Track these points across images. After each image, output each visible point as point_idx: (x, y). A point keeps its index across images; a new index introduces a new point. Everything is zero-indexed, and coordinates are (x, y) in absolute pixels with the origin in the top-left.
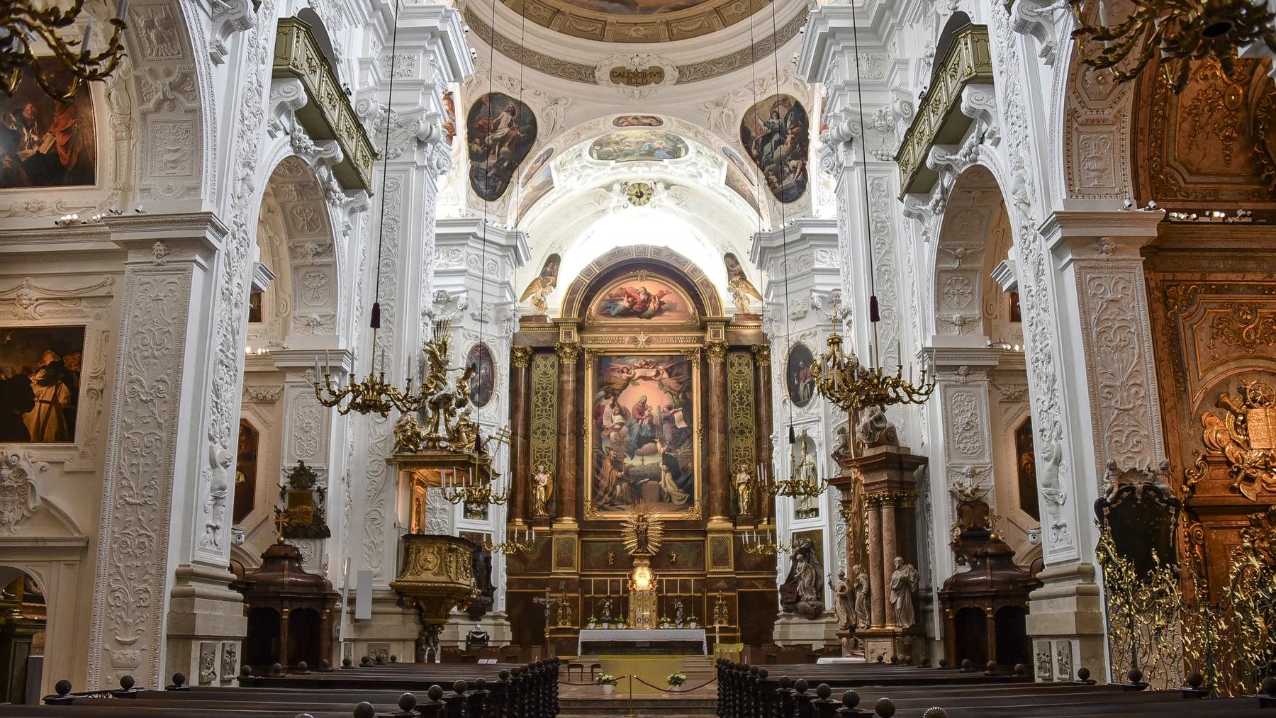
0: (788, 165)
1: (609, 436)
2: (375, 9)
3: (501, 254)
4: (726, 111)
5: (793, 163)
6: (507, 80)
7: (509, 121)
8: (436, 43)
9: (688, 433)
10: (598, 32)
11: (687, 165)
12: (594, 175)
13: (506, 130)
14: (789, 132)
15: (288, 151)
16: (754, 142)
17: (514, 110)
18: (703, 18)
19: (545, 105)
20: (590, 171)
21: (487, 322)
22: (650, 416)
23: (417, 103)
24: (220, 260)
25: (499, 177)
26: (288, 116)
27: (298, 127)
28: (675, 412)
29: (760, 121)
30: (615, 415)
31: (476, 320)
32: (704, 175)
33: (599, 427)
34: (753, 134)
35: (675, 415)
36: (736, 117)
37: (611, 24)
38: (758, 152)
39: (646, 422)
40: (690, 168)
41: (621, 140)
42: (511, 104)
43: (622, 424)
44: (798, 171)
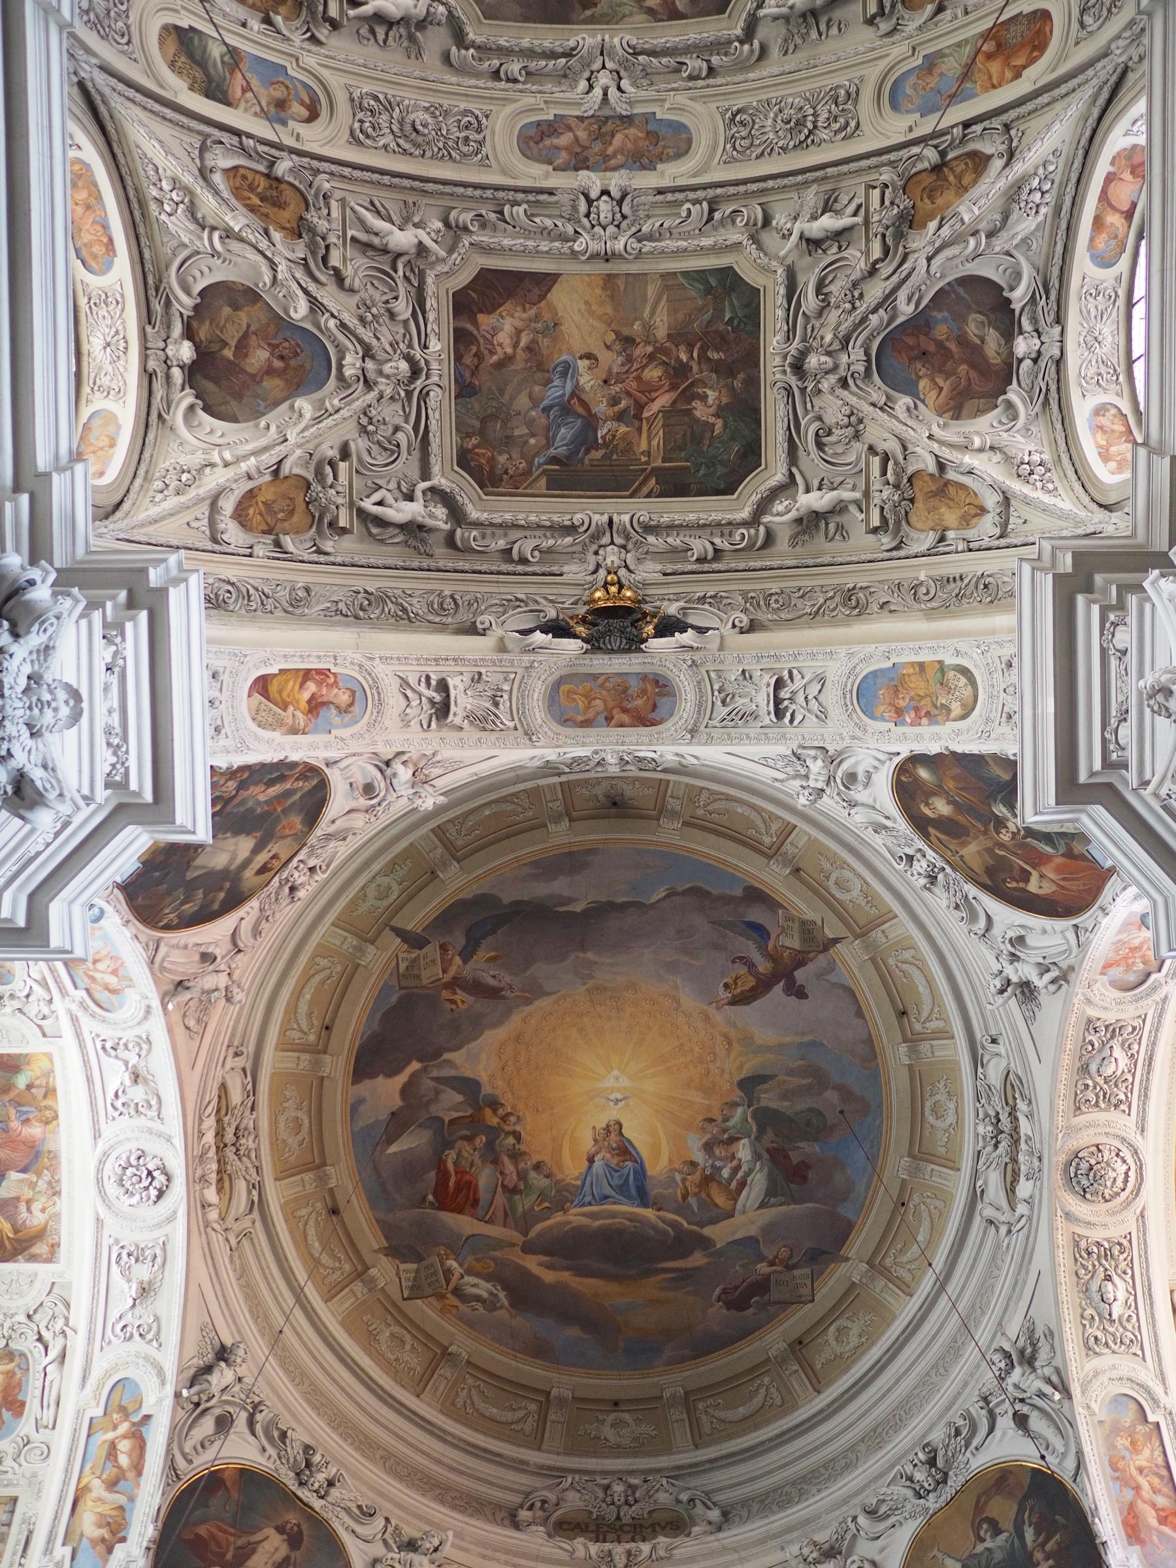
2: (17, 488)
6: (297, 1445)
14: (1038, 1555)
17: (300, 1532)
18: (766, 1380)
37: (561, 1401)
42: (292, 1518)
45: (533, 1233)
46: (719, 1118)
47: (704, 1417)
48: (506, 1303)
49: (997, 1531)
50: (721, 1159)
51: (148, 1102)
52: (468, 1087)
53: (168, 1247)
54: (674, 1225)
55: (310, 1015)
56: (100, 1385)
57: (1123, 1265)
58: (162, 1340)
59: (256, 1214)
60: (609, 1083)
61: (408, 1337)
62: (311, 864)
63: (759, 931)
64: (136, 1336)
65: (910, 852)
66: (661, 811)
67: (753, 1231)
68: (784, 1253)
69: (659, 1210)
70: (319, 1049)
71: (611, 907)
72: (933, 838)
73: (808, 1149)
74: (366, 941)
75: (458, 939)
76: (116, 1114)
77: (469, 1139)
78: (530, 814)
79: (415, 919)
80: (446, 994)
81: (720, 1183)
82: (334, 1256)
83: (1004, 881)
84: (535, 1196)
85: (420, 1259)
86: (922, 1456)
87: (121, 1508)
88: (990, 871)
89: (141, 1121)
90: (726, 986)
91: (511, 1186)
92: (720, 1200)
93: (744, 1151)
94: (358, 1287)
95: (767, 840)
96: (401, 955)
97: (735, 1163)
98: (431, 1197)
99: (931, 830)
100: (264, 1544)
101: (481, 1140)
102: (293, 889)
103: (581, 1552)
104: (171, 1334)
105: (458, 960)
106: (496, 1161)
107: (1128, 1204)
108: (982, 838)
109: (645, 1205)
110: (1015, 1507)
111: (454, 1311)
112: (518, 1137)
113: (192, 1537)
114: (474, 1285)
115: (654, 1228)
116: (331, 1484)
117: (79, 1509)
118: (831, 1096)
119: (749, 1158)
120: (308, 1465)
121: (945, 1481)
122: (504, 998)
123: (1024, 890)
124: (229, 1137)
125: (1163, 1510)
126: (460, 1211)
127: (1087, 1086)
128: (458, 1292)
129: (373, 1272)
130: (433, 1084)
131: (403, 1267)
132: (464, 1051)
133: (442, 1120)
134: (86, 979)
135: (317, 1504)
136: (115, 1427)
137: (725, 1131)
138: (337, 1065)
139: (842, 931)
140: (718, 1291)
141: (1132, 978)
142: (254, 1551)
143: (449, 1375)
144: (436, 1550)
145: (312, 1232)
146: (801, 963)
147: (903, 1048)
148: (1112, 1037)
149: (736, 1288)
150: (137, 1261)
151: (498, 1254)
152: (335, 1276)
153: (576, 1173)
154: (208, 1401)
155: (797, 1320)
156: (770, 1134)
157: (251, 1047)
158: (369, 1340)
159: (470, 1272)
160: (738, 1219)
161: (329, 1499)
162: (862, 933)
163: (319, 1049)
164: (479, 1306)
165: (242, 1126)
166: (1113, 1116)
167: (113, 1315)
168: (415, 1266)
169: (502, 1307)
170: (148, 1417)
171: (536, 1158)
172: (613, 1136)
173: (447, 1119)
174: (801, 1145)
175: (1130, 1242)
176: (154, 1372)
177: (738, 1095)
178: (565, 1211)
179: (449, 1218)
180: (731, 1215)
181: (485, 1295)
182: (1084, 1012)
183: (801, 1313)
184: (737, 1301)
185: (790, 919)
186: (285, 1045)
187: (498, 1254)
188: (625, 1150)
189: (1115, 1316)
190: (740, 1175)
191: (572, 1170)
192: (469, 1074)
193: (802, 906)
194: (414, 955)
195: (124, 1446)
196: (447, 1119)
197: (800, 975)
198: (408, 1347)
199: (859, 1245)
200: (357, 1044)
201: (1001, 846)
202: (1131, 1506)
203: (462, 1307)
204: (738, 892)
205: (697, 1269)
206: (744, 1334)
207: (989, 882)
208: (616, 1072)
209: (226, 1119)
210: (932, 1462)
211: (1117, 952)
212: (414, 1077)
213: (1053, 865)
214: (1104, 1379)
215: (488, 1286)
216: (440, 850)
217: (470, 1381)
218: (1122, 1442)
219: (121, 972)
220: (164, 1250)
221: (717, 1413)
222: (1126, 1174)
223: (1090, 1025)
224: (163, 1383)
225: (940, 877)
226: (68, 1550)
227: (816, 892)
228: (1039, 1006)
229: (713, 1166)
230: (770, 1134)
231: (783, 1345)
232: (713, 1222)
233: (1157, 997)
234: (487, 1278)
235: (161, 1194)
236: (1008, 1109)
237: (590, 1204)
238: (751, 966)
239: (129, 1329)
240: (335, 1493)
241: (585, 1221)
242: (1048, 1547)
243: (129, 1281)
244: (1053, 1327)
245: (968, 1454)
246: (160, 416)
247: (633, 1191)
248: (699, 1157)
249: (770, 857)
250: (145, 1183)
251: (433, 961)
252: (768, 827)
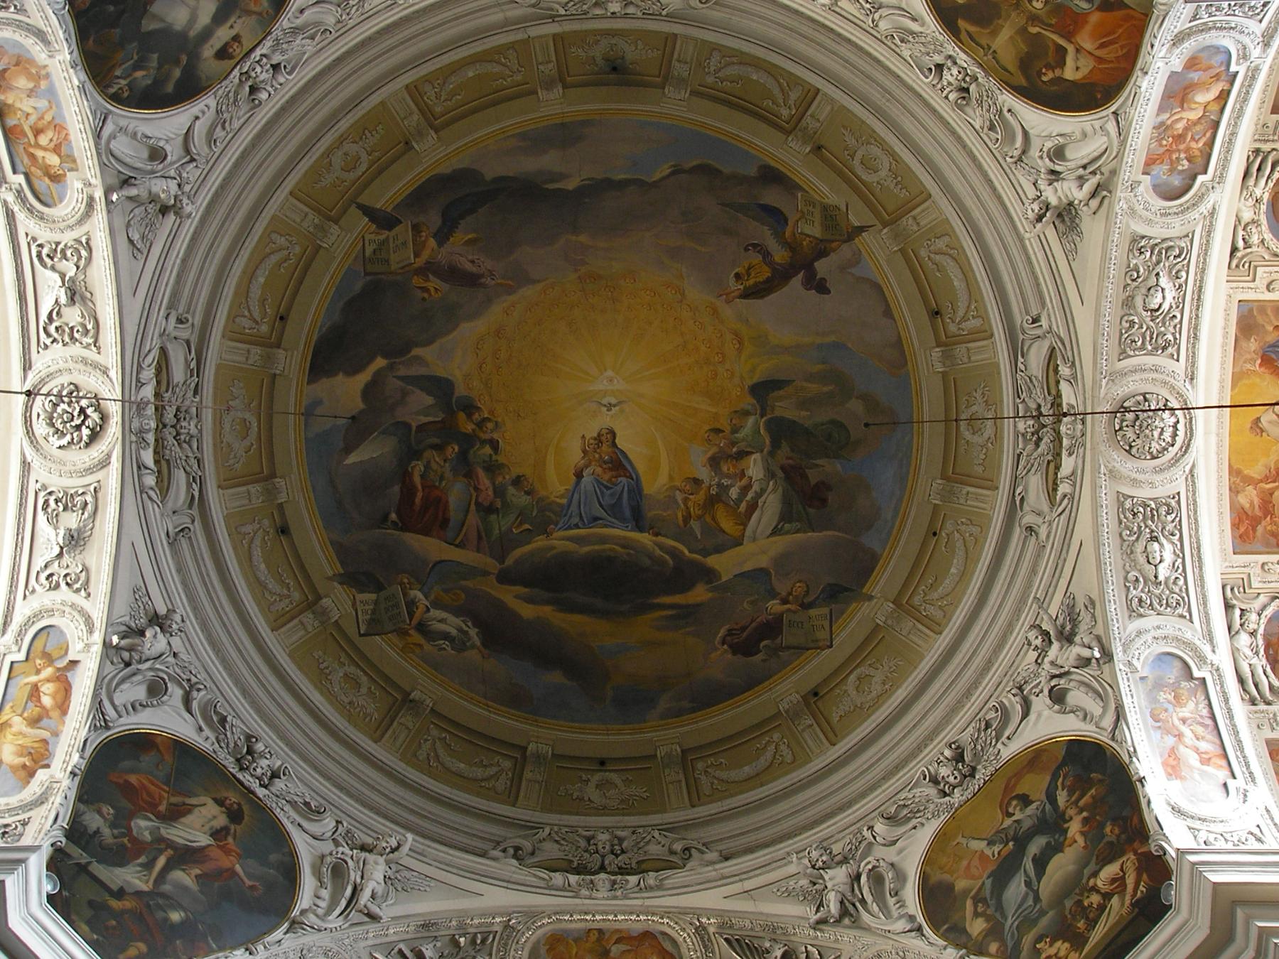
0: (1094, 889)
5: (1111, 870)
10: (501, 784)
13: (203, 840)
14: (1071, 812)
16: (969, 903)
18: (776, 736)
36: (901, 877)
37: (538, 757)
38: (988, 918)
42: (233, 798)
44: (1130, 881)
45: (509, 561)
46: (728, 429)
47: (703, 777)
48: (477, 641)
49: (1025, 800)
50: (728, 476)
51: (84, 326)
52: (440, 387)
53: (100, 495)
54: (673, 553)
55: (263, 302)
56: (21, 634)
57: (1170, 527)
58: (91, 590)
59: (195, 512)
60: (602, 385)
61: (364, 679)
62: (276, 59)
63: (776, 217)
64: (63, 585)
65: (938, 59)
66: (666, 78)
67: (763, 562)
68: (799, 589)
69: (656, 535)
70: (272, 343)
71: (608, 185)
72: (964, 36)
73: (825, 468)
74: (329, 219)
75: (433, 219)
76: (48, 341)
77: (439, 448)
78: (519, 78)
79: (386, 196)
80: (417, 281)
81: (727, 505)
82: (282, 582)
83: (1040, 74)
84: (512, 517)
85: (379, 588)
86: (947, 753)
87: (45, 741)
88: (1025, 64)
89: (76, 350)
90: (738, 276)
91: (486, 504)
92: (727, 524)
93: (755, 467)
94: (308, 618)
95: (785, 113)
96: (367, 237)
97: (744, 482)
98: (393, 516)
99: (962, 23)
100: (202, 809)
101: (453, 449)
102: (253, 90)
104: (101, 584)
105: (432, 243)
106: (469, 475)
107: (1176, 461)
108: (1013, 14)
109: (640, 529)
110: (1048, 778)
111: (418, 651)
112: (495, 445)
113: (121, 781)
114: (442, 621)
115: (651, 556)
116: (275, 775)
118: (855, 406)
119: (761, 476)
120: (250, 752)
121: (972, 775)
122: (484, 286)
123: (1060, 80)
124: (169, 416)
125: (1206, 753)
126: (426, 532)
127: (1132, 323)
128: (422, 628)
129: (326, 602)
130: (400, 383)
131: (360, 597)
132: (436, 346)
133: (407, 426)
134: (26, 160)
135: (261, 792)
136: (38, 672)
137: (733, 444)
138: (292, 361)
139: (869, 218)
140: (722, 632)
141: (1176, 181)
142: (189, 812)
143: (410, 725)
144: (393, 851)
145: (257, 553)
146: (822, 254)
147: (937, 353)
148: (1158, 262)
149: (743, 629)
150: (65, 509)
151: (469, 584)
152: (282, 605)
153: (562, 489)
154: (140, 662)
155: (812, 668)
156: (785, 450)
157: (198, 320)
158: (321, 678)
159: (437, 604)
160: (747, 547)
161: (273, 789)
162: (892, 220)
163: (272, 343)
164: (445, 644)
165: (183, 409)
166: (1161, 360)
167: (38, 563)
168: (373, 596)
169: (473, 646)
170: (74, 663)
171: (515, 471)
172: (605, 448)
173: (414, 425)
174: (819, 462)
175: (1179, 502)
176: (81, 621)
177: (749, 402)
178: (548, 534)
179: (415, 541)
180: (738, 542)
181: (454, 632)
182: (1128, 226)
183: (815, 662)
184: (744, 645)
185: (812, 203)
186: (232, 333)
187: (469, 584)
188: (618, 464)
189: (1161, 578)
190: (749, 497)
191: (556, 485)
192: (441, 373)
193: (826, 190)
194: (382, 237)
195: (48, 688)
196: (414, 425)
197: (821, 267)
198: (364, 690)
199: (883, 582)
200: (315, 338)
201: (1034, 19)
202: (1173, 752)
203: (428, 647)
204: (752, 171)
205: (698, 605)
206: (752, 682)
207: (1024, 82)
208: (610, 373)
209: (167, 395)
210: (959, 757)
211: (1159, 140)
212: (377, 374)
213: (1088, 28)
214: (1149, 637)
215: (458, 621)
216: (415, 117)
217: (435, 732)
218: (1165, 696)
219: (64, 150)
220: (96, 498)
221: (718, 773)
222: (1175, 427)
223: (1137, 244)
225: (973, 88)
227: (840, 174)
228: (1080, 234)
229: (719, 485)
230: (785, 450)
231: (796, 698)
232: (719, 550)
233: (1204, 208)
234: (457, 612)
235: (95, 436)
236: (1049, 399)
237: (577, 526)
238: (766, 255)
239: (55, 578)
240: (279, 784)
241: (571, 546)
242: (1081, 803)
243: (56, 528)
244: (1094, 596)
245: (999, 746)
247: (628, 513)
248: (704, 473)
249: (788, 133)
250: (77, 422)
251: (404, 244)
252: (786, 97)
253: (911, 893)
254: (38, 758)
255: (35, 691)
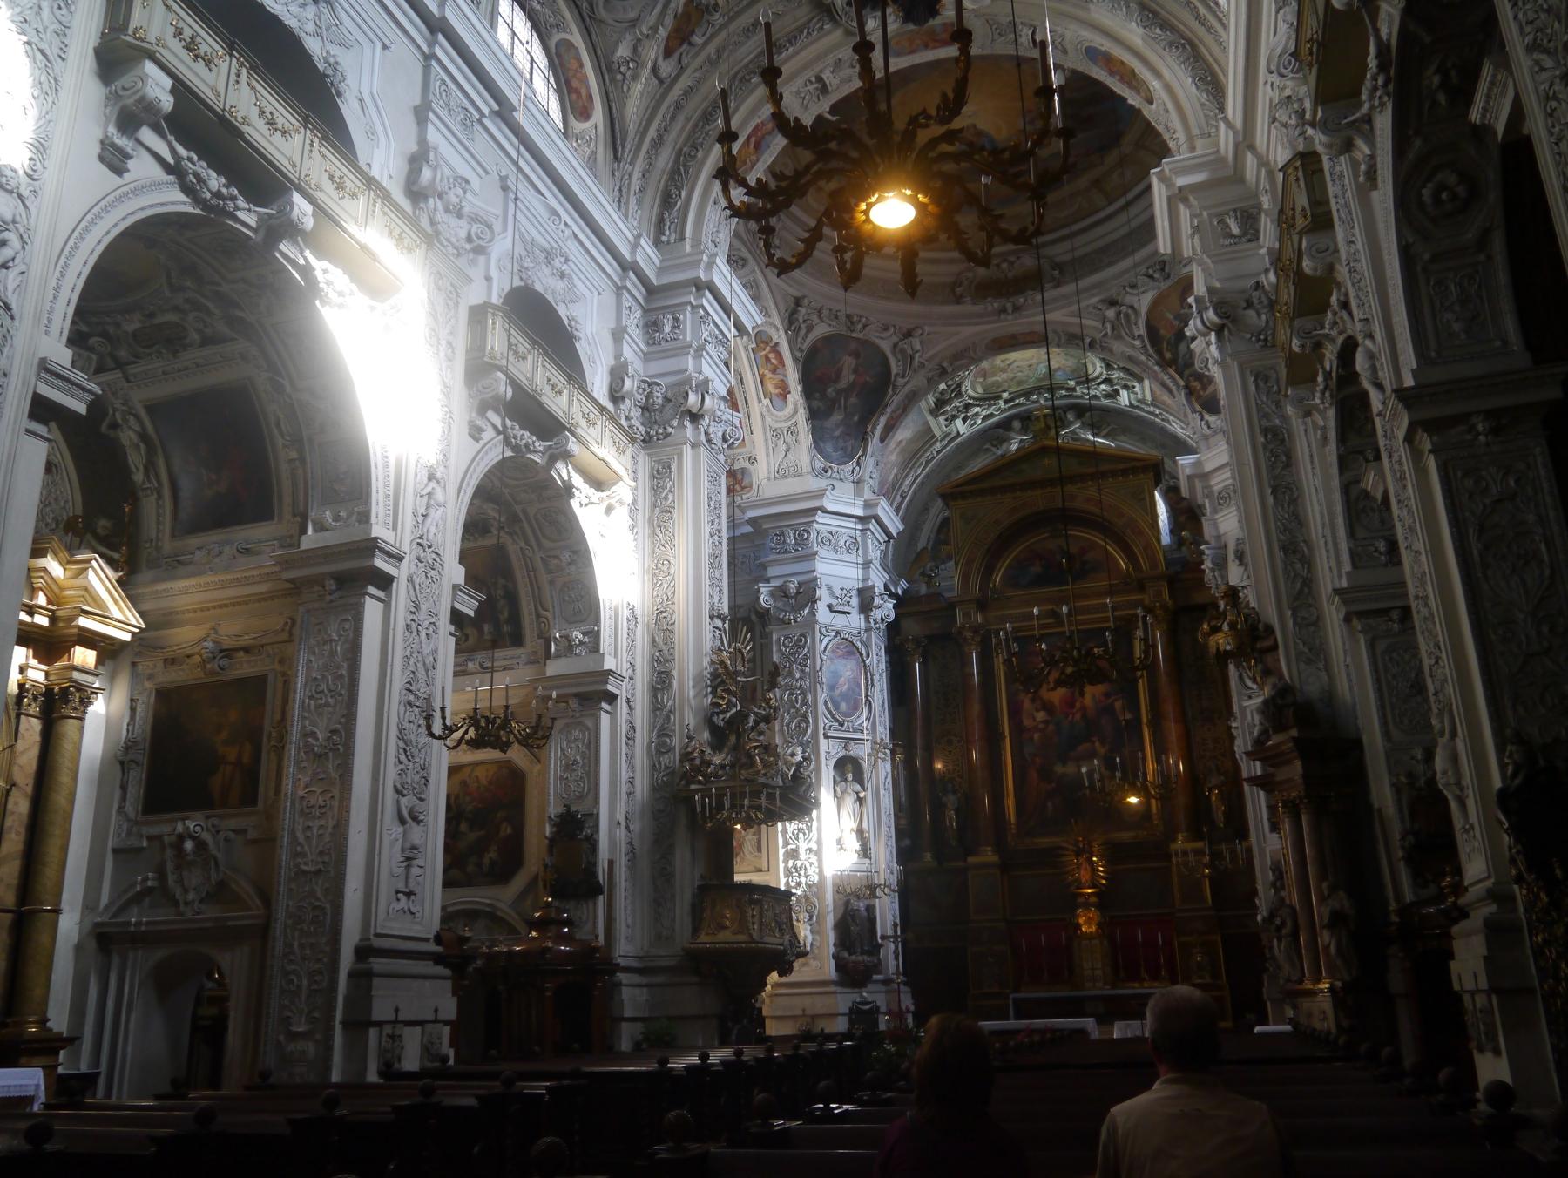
1: (1032, 738)
3: (859, 527)
4: (1124, 309)
7: (853, 366)
8: (703, 296)
9: (1135, 726)
11: (1099, 384)
12: (984, 413)
13: (852, 377)
15: (496, 453)
19: (895, 339)
20: (977, 409)
21: (849, 613)
22: (1083, 708)
23: (686, 370)
24: (401, 590)
25: (848, 434)
26: (497, 411)
27: (509, 423)
28: (1116, 700)
29: (1171, 317)
30: (1037, 710)
31: (835, 612)
32: (1124, 393)
33: (1018, 728)
34: (1162, 332)
35: (1118, 705)
38: (1172, 354)
39: (1078, 716)
40: (1103, 387)
41: (1009, 365)
42: (853, 345)
43: (1046, 722)
87: (782, 380)
103: (990, 308)
117: (765, 383)
120: (852, 323)
170: (777, 344)
195: (771, 356)
224: (778, 330)
226: (768, 400)
246: (590, 17)
253: (1142, 323)
254: (784, 392)
255: (767, 359)
